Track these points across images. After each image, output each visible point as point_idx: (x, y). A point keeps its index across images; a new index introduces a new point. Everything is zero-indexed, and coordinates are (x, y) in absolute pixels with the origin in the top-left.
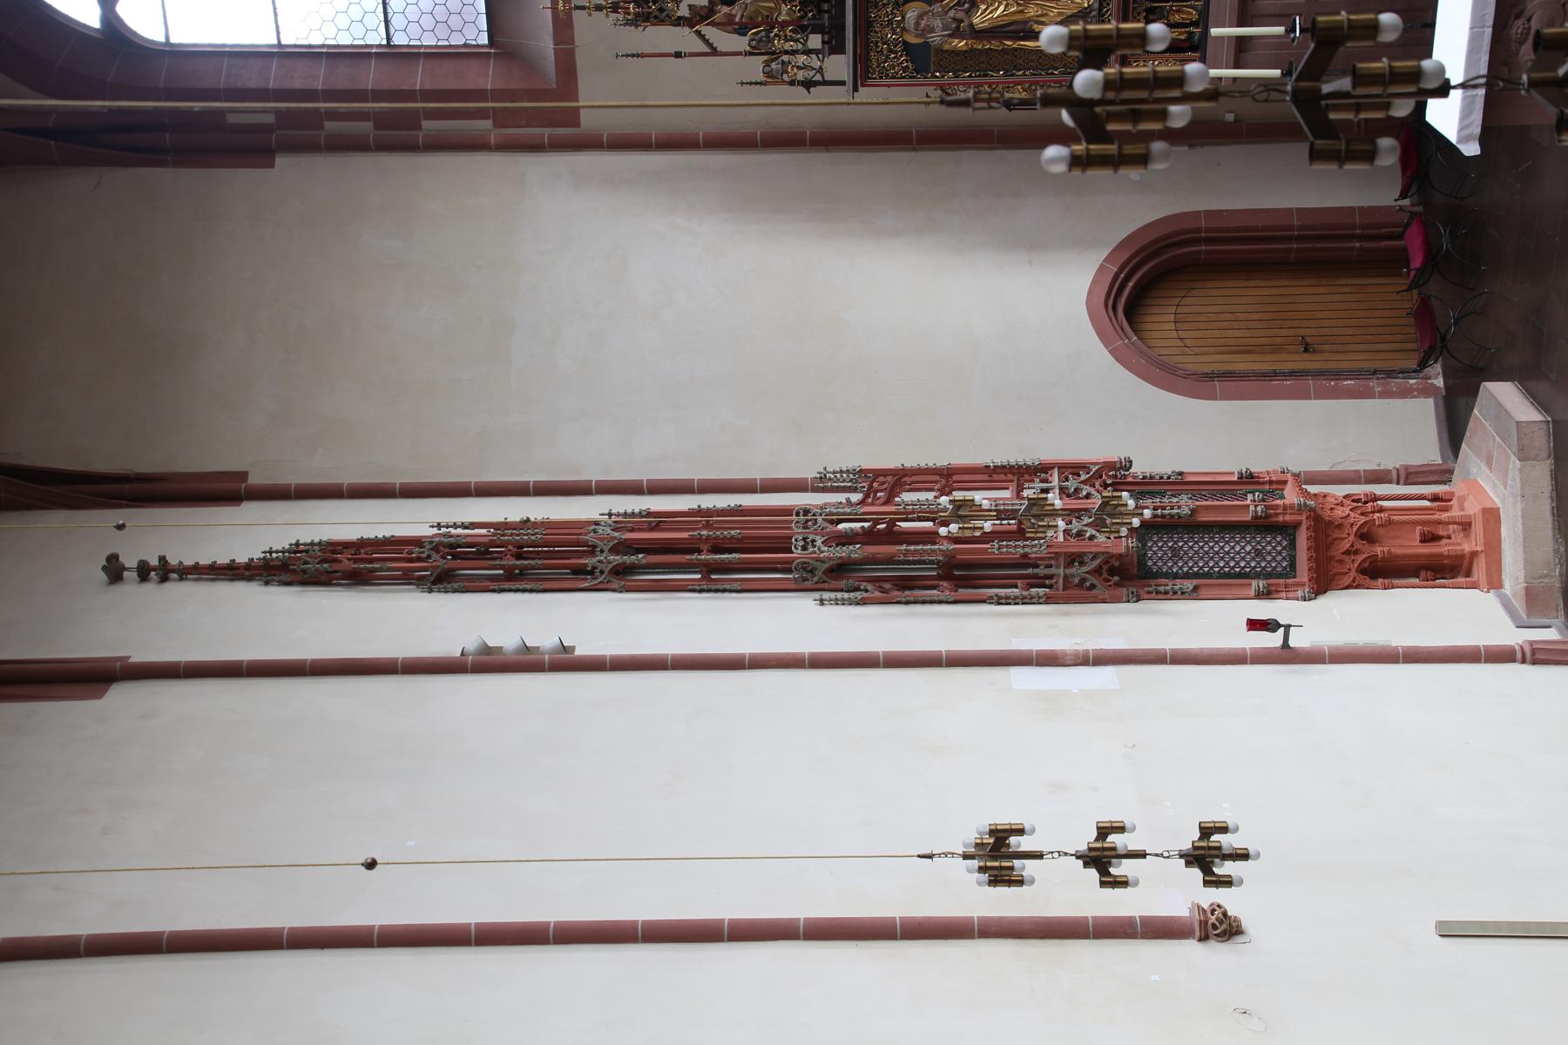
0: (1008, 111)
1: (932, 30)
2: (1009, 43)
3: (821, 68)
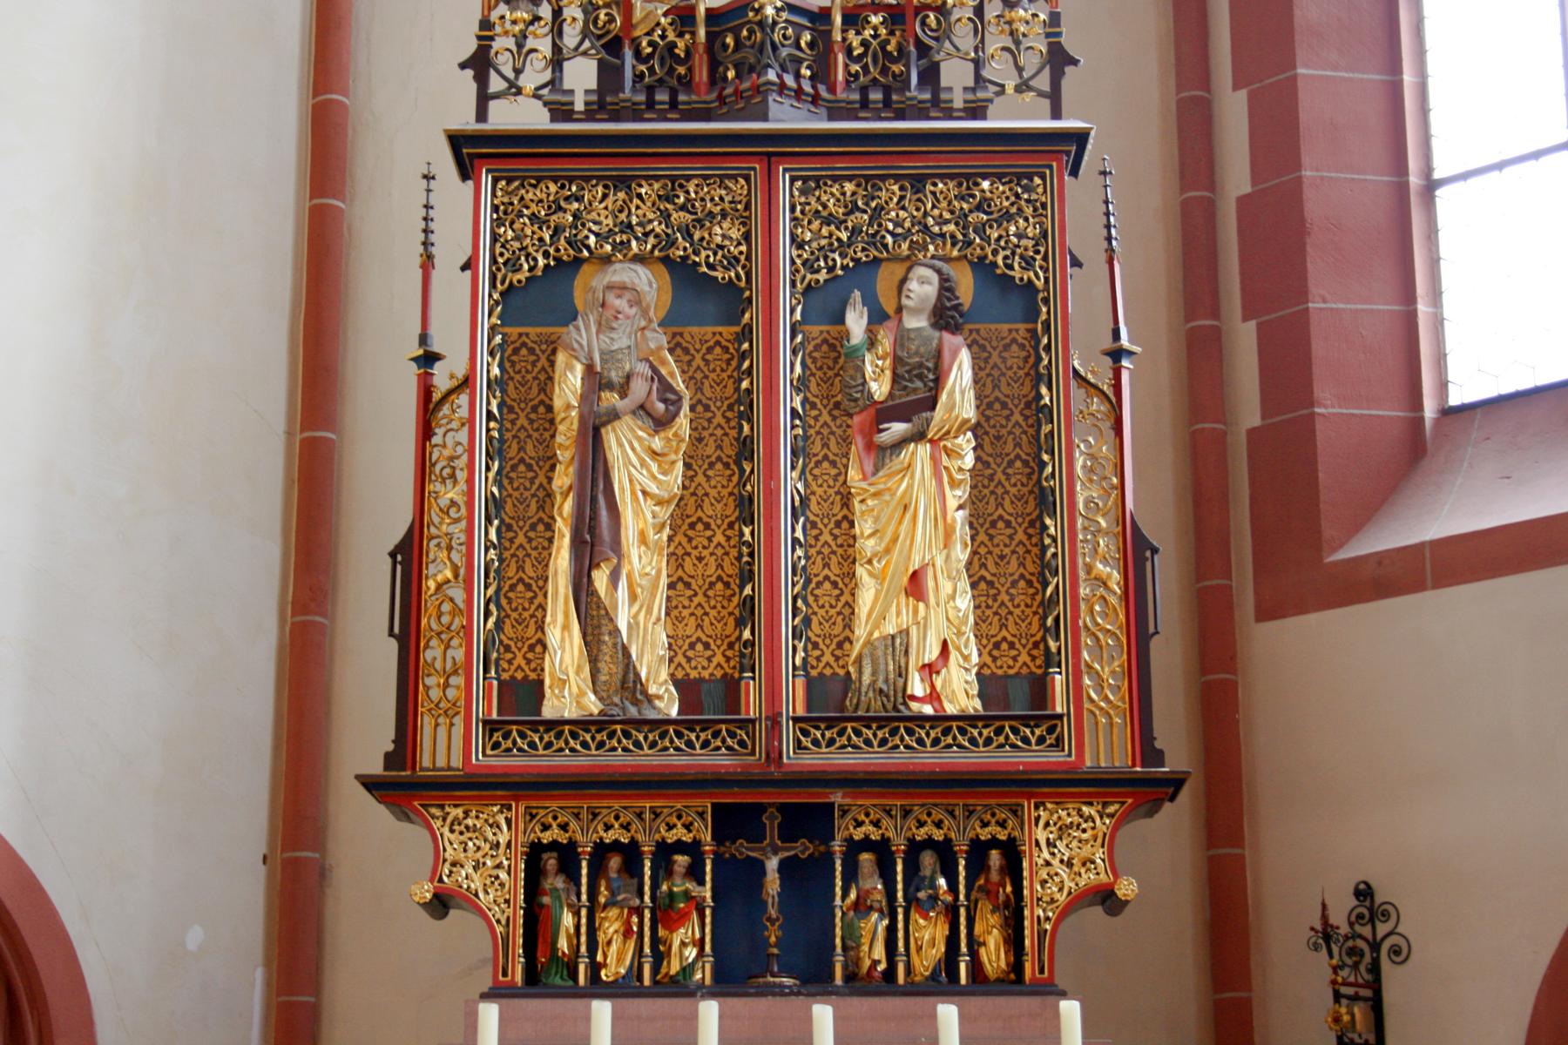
0: (391, 547)
2: (568, 506)
3: (519, 92)
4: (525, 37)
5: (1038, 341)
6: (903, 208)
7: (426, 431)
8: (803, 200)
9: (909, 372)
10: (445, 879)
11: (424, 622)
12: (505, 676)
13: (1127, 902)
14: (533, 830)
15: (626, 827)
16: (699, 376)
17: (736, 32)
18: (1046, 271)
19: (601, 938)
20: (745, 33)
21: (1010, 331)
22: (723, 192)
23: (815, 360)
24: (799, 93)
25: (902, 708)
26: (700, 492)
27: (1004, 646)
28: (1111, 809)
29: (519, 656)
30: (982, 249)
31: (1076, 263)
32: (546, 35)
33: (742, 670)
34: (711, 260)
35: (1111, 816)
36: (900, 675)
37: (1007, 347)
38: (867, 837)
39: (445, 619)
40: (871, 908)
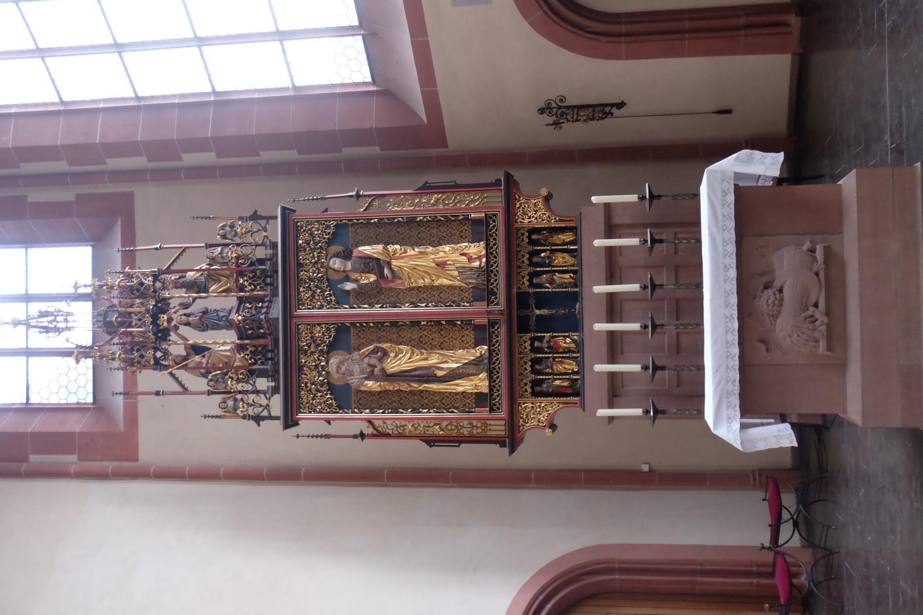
0: (429, 447)
1: (351, 374)
2: (415, 385)
3: (268, 405)
4: (249, 403)
5: (355, 223)
6: (309, 270)
7: (387, 436)
8: (306, 305)
9: (367, 268)
10: (544, 425)
11: (454, 435)
12: (474, 406)
13: (549, 192)
14: (527, 395)
15: (525, 363)
16: (368, 341)
17: (246, 330)
18: (330, 221)
19: (563, 371)
20: (247, 327)
21: (352, 233)
22: (304, 333)
23: (362, 301)
24: (268, 307)
25: (483, 269)
26: (409, 339)
27: (462, 234)
28: (517, 197)
29: (467, 401)
30: (323, 243)
31: (326, 210)
32: (248, 396)
33: (471, 324)
34: (328, 337)
35: (520, 197)
36: (472, 269)
37: (357, 234)
38: (528, 280)
39: (453, 428)
40: (552, 279)
